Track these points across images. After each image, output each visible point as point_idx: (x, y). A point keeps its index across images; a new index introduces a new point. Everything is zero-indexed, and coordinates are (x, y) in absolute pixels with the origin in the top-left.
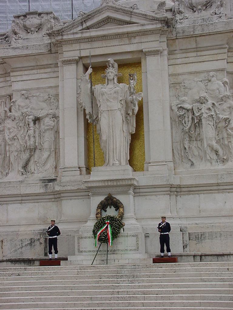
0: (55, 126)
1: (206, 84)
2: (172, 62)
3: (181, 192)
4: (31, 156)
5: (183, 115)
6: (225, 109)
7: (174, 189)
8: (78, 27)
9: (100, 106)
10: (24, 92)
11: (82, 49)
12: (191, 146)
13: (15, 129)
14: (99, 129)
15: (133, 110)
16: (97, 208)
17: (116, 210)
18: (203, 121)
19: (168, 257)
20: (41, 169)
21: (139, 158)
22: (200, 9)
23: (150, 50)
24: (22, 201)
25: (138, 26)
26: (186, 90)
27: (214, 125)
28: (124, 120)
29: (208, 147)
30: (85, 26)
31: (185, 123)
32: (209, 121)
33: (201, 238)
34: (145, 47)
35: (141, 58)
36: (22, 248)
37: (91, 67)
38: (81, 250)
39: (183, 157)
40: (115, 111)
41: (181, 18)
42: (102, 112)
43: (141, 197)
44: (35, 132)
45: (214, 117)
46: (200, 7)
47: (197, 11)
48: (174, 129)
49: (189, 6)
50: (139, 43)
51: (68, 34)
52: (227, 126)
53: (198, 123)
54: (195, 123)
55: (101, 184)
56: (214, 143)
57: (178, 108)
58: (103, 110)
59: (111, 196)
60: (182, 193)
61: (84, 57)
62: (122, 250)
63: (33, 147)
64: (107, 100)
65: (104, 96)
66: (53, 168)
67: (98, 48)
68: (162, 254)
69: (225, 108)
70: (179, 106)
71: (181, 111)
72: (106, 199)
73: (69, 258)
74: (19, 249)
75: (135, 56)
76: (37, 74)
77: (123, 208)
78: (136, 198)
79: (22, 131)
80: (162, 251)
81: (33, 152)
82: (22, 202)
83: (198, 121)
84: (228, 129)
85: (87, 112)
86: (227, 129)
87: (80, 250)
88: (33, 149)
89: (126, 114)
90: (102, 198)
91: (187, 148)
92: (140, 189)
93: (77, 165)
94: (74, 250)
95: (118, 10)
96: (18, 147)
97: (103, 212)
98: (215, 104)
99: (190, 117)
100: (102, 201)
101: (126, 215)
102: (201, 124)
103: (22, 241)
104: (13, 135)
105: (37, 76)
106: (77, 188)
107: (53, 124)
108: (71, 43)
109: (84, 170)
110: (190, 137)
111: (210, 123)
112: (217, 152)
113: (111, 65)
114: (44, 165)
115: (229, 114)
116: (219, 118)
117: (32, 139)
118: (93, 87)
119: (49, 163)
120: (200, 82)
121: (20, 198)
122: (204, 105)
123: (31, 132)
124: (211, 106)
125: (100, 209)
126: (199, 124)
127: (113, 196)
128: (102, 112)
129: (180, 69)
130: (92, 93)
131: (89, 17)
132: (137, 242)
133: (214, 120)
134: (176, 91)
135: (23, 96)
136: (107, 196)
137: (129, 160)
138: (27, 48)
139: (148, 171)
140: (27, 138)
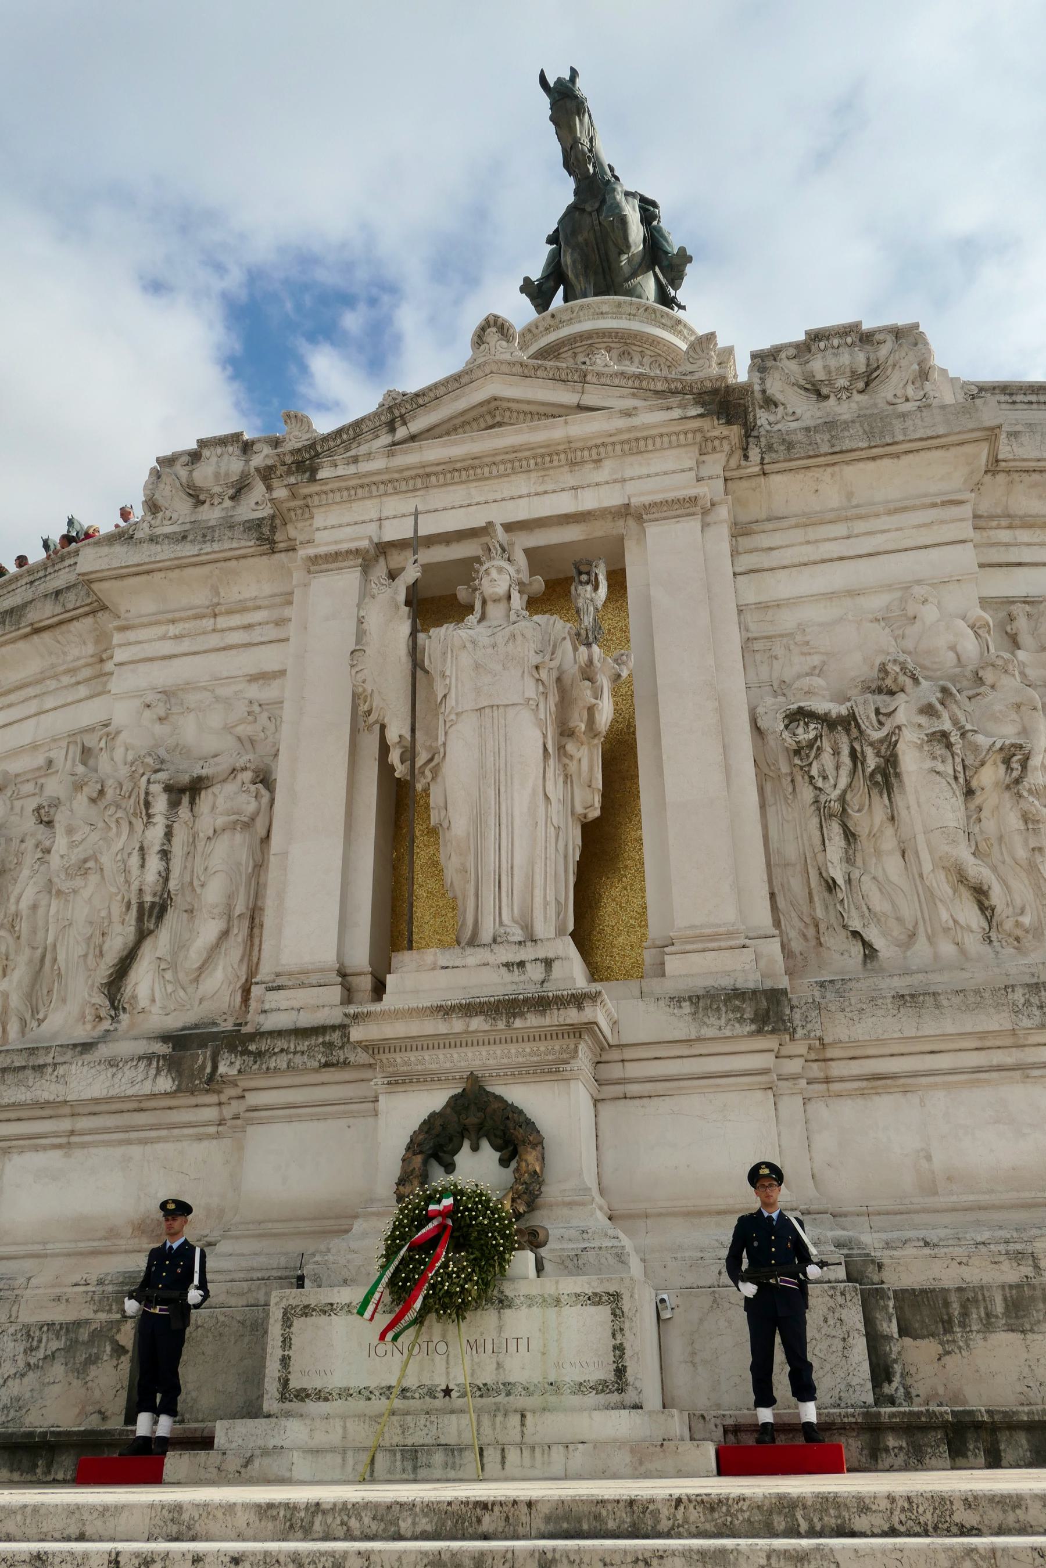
0: (258, 813)
2: (747, 561)
3: (827, 1080)
4: (142, 935)
5: (811, 744)
6: (1000, 711)
8: (377, 437)
9: (445, 696)
11: (387, 518)
12: (856, 874)
14: (442, 805)
15: (591, 710)
16: (408, 1149)
17: (504, 1162)
19: (800, 1440)
20: (182, 993)
21: (620, 939)
23: (658, 497)
27: (956, 778)
28: (550, 750)
29: (942, 875)
30: (401, 432)
31: (825, 778)
32: (935, 758)
33: (963, 1325)
34: (639, 493)
35: (621, 540)
36: (23, 1375)
38: (295, 1383)
39: (822, 926)
40: (511, 712)
42: (453, 717)
44: (169, 835)
46: (842, 382)
47: (832, 395)
48: (771, 811)
50: (615, 481)
52: (1017, 781)
54: (870, 770)
56: (964, 853)
57: (786, 716)
58: (460, 710)
59: (482, 1089)
60: (835, 1087)
61: (392, 544)
62: (526, 1389)
63: (155, 895)
66: (233, 991)
67: (453, 508)
68: (765, 1415)
71: (800, 730)
73: (223, 1432)
74: (10, 1383)
75: (599, 530)
76: (214, 630)
77: (539, 1148)
79: (124, 837)
80: (764, 1396)
81: (153, 921)
82: (69, 1143)
85: (392, 736)
87: (294, 1384)
88: (153, 904)
89: (562, 734)
90: (434, 1100)
91: (840, 881)
92: (626, 1064)
93: (328, 957)
94: (255, 1377)
95: (532, 373)
99: (845, 751)
100: (433, 1116)
101: (552, 1191)
102: (898, 775)
103: (29, 1336)
105: (214, 641)
106: (323, 1061)
107: (252, 807)
108: (345, 499)
109: (365, 983)
111: (940, 767)
112: (980, 894)
114: (196, 980)
116: (976, 748)
117: (154, 864)
118: (421, 636)
119: (220, 968)
121: (66, 1125)
123: (155, 834)
124: (937, 699)
125: (421, 1152)
126: (886, 776)
127: (489, 1089)
128: (453, 717)
129: (781, 586)
131: (421, 402)
132: (614, 1335)
136: (460, 1090)
139: (663, 975)
140: (135, 860)
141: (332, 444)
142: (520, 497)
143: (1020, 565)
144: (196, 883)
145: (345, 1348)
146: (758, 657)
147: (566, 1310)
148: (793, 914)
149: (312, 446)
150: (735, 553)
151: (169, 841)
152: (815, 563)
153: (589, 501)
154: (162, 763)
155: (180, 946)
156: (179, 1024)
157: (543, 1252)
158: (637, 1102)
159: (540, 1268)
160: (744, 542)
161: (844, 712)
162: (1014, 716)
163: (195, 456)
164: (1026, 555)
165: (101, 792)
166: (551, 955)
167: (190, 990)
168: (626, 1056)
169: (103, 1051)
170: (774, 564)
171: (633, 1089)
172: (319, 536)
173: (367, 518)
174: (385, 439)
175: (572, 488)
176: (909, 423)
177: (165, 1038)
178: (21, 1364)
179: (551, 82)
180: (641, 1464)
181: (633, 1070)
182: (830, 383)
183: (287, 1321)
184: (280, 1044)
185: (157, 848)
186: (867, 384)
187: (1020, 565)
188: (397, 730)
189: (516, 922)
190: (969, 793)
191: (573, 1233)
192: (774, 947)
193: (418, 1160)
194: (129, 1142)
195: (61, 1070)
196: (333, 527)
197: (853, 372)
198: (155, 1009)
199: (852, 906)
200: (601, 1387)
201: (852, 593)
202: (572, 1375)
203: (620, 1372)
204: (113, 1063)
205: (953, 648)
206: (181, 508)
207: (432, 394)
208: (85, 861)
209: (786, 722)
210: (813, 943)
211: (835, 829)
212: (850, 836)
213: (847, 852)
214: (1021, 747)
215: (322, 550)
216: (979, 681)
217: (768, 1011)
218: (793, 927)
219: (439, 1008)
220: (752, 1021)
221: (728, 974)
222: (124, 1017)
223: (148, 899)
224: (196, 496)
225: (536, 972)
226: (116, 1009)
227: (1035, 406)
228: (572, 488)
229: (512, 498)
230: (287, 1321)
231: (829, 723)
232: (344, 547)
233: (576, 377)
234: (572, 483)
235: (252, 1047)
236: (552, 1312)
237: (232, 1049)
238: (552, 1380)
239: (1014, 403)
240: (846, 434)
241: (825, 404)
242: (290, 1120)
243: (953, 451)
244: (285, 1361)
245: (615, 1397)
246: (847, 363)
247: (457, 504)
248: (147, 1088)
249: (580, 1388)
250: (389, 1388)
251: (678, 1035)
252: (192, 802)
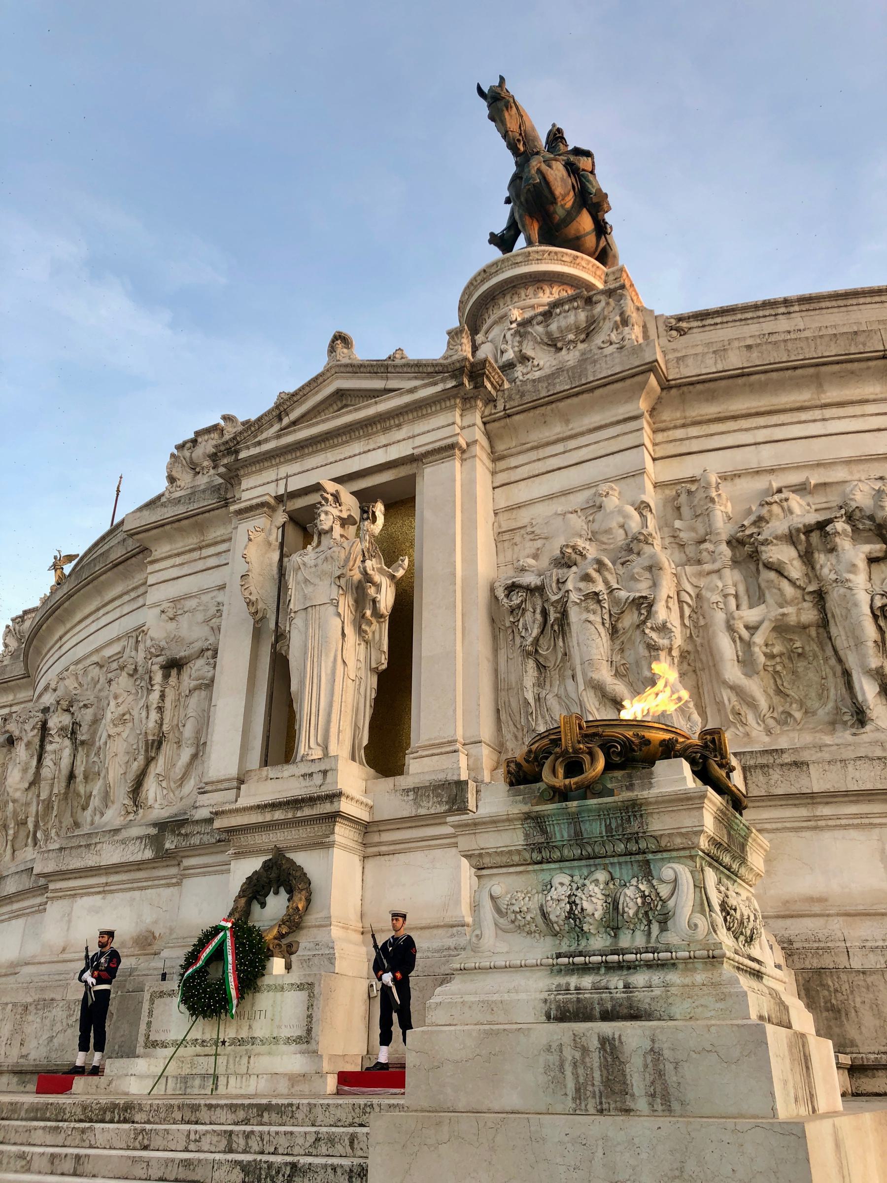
1: (591, 518)
2: (502, 478)
4: (149, 761)
5: (519, 606)
6: (637, 573)
8: (272, 426)
10: (165, 605)
13: (131, 697)
15: (374, 601)
17: (289, 900)
18: (574, 615)
20: (172, 795)
22: (571, 341)
24: (107, 888)
25: (401, 394)
26: (539, 543)
30: (286, 421)
31: (526, 629)
32: (589, 612)
38: (152, 1038)
39: (525, 730)
41: (525, 371)
43: (382, 858)
44: (163, 696)
45: (600, 598)
46: (571, 337)
49: (546, 340)
50: (409, 438)
51: (248, 448)
52: (644, 622)
53: (557, 624)
56: (605, 675)
62: (261, 1041)
63: (154, 735)
64: (306, 581)
65: (300, 573)
69: (636, 570)
70: (510, 582)
72: (266, 866)
73: (112, 1067)
76: (200, 559)
78: (371, 864)
81: (154, 751)
83: (558, 615)
84: (647, 631)
86: (643, 631)
87: (152, 1038)
88: (153, 741)
96: (132, 740)
97: (256, 907)
98: (607, 561)
100: (255, 873)
102: (569, 624)
104: (121, 710)
105: (200, 565)
110: (541, 667)
111: (592, 617)
113: (329, 496)
114: (181, 785)
115: (650, 587)
116: (616, 602)
117: (154, 715)
118: (285, 560)
120: (574, 516)
121: (103, 880)
122: (574, 569)
123: (155, 696)
124: (594, 569)
127: (288, 855)
131: (295, 399)
133: (602, 607)
134: (513, 549)
135: (163, 615)
137: (366, 748)
138: (179, 501)
141: (246, 434)
142: (355, 455)
144: (180, 725)
145: (172, 1018)
146: (506, 544)
147: (286, 994)
148: (511, 723)
149: (234, 438)
150: (494, 473)
151: (163, 700)
152: (543, 474)
153: (394, 453)
154: (162, 650)
156: (167, 815)
157: (294, 958)
158: (387, 857)
159: (288, 967)
160: (502, 465)
161: (539, 583)
162: (647, 575)
163: (194, 442)
164: (695, 446)
165: (136, 670)
166: (328, 768)
167: (177, 793)
168: (382, 828)
169: (124, 834)
170: (517, 478)
171: (384, 849)
172: (245, 496)
173: (269, 480)
174: (276, 427)
175: (385, 446)
176: (598, 366)
177: (155, 825)
178: (65, 1024)
179: (486, 90)
180: (293, 1087)
182: (563, 338)
183: (152, 1001)
184: (197, 828)
185: (155, 706)
186: (588, 335)
189: (318, 744)
191: (312, 945)
193: (243, 901)
194: (133, 889)
195: (99, 847)
196: (252, 488)
197: (577, 328)
198: (157, 806)
199: (539, 717)
200: (299, 1040)
201: (565, 493)
202: (286, 1033)
203: (309, 1031)
204: (123, 842)
205: (622, 526)
206: (185, 479)
207: (301, 393)
208: (124, 715)
209: (506, 592)
210: (520, 742)
211: (531, 664)
213: (538, 679)
214: (645, 598)
215: (242, 505)
216: (630, 551)
217: (456, 795)
218: (510, 732)
219: (258, 807)
220: (447, 803)
221: (443, 771)
222: (141, 811)
223: (150, 738)
224: (195, 468)
225: (318, 779)
226: (137, 806)
227: (719, 326)
228: (385, 446)
229: (350, 457)
230: (152, 1001)
231: (531, 590)
232: (254, 502)
233: (382, 370)
234: (385, 442)
235: (183, 832)
236: (279, 994)
237: (173, 832)
238: (275, 1036)
239: (704, 326)
240: (558, 380)
241: (559, 354)
242: (204, 874)
243: (628, 382)
244: (149, 1024)
245: (305, 1046)
246: (572, 322)
247: (319, 465)
248: (139, 857)
249: (288, 1041)
250: (197, 1040)
251: (406, 814)
252: (179, 673)
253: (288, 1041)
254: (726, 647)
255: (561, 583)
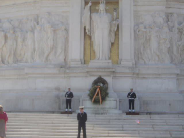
7: (135, 76)
15: (114, 29)
37: (91, 2)
55: (96, 70)
68: (130, 110)
85: (87, 28)
90: (95, 78)
130: (91, 18)
139: (121, 64)
143: (171, 8)
155: (56, 53)
181: (117, 75)
187: (171, 8)
188: (88, 28)
190: (159, 43)
192: (134, 61)
200: (115, 108)
212: (144, 47)
249: (113, 108)
253: (113, 108)
254: (175, 48)
255: (150, 32)
